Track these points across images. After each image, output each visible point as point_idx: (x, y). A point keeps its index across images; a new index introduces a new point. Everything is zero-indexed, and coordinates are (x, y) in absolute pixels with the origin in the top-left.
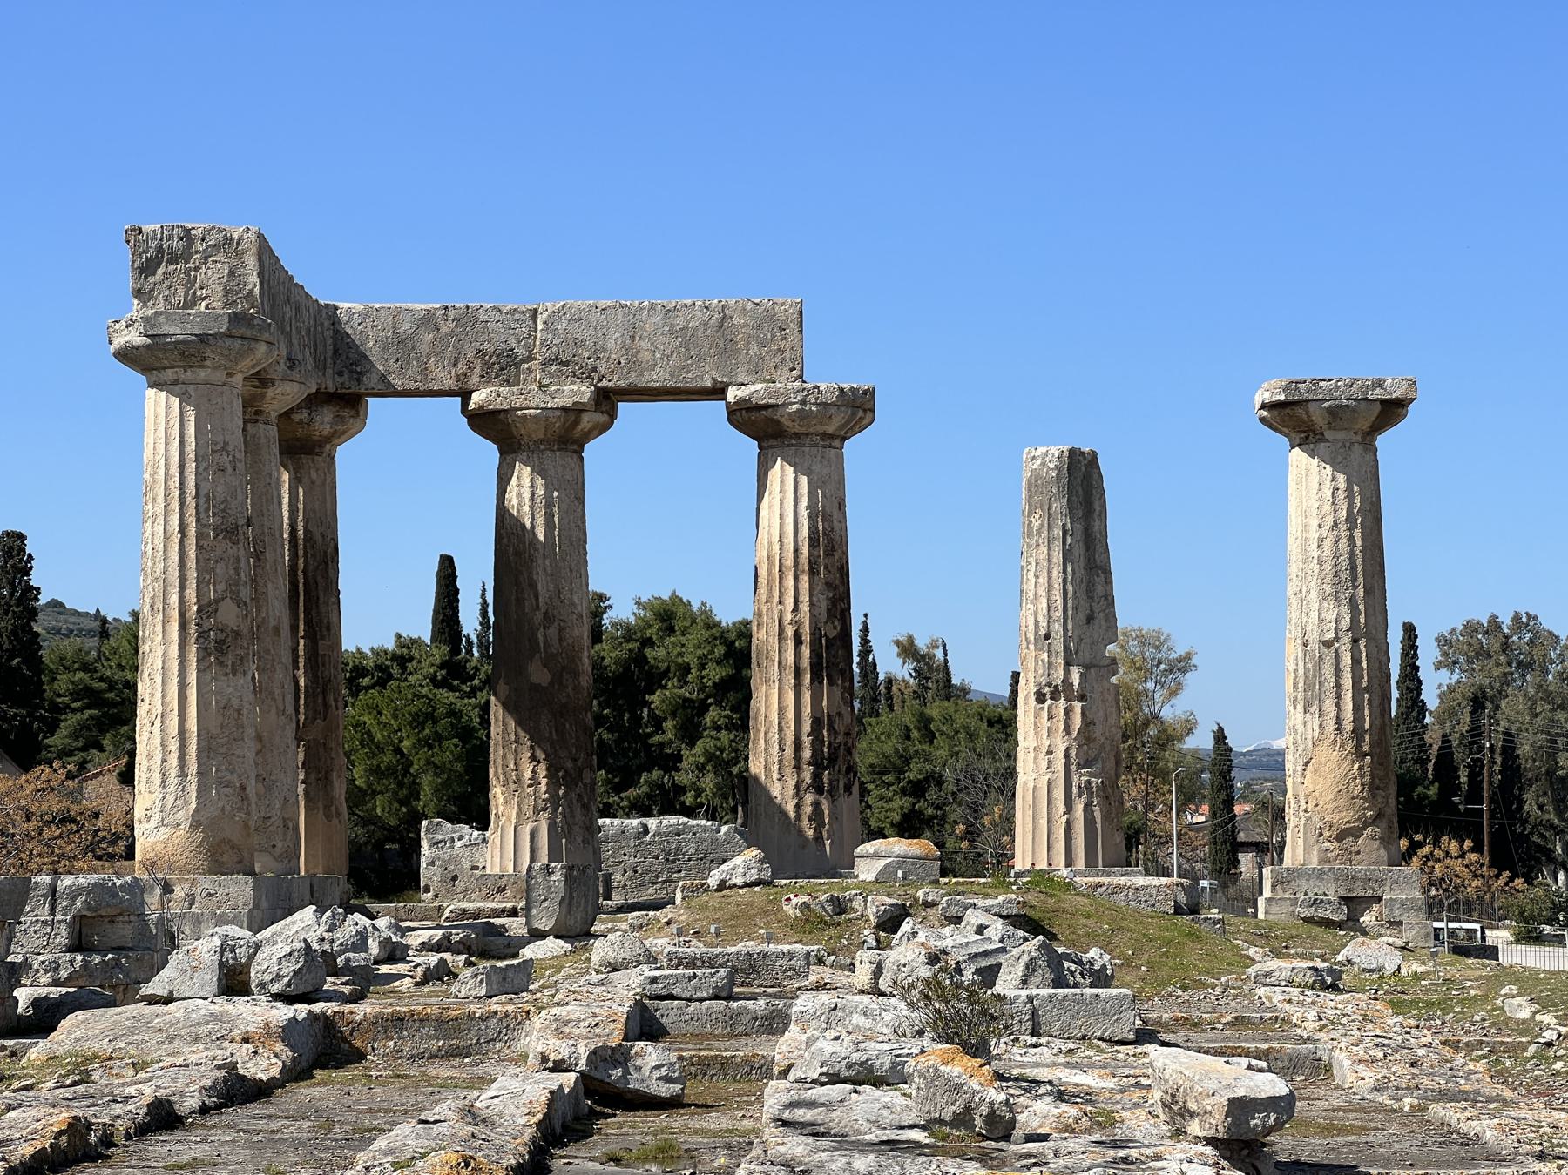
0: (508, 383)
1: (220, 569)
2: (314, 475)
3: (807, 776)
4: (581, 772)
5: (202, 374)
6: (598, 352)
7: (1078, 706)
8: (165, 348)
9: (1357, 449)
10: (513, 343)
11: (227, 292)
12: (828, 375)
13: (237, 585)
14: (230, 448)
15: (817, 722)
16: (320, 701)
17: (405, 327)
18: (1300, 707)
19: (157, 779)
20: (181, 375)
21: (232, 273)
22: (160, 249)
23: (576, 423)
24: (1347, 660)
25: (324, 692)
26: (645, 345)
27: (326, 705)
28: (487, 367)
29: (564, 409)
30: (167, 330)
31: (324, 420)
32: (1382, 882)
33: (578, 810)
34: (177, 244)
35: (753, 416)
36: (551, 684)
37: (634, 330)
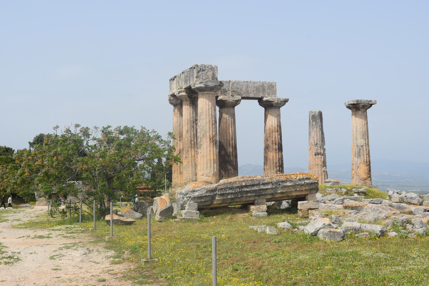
0: (225, 95)
3: (278, 169)
5: (212, 92)
6: (241, 90)
7: (323, 157)
8: (208, 88)
11: (212, 77)
12: (280, 95)
18: (356, 157)
19: (205, 168)
20: (208, 92)
21: (213, 74)
22: (201, 69)
24: (365, 149)
26: (250, 89)
29: (236, 100)
30: (209, 84)
34: (204, 68)
35: (268, 103)
37: (248, 87)
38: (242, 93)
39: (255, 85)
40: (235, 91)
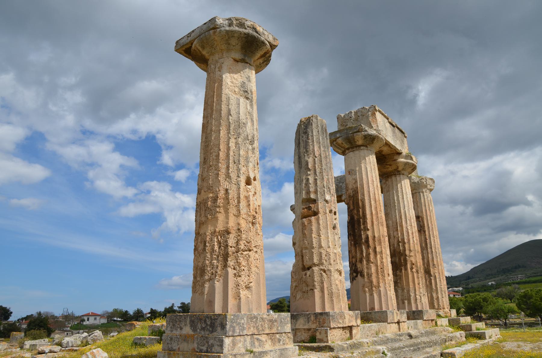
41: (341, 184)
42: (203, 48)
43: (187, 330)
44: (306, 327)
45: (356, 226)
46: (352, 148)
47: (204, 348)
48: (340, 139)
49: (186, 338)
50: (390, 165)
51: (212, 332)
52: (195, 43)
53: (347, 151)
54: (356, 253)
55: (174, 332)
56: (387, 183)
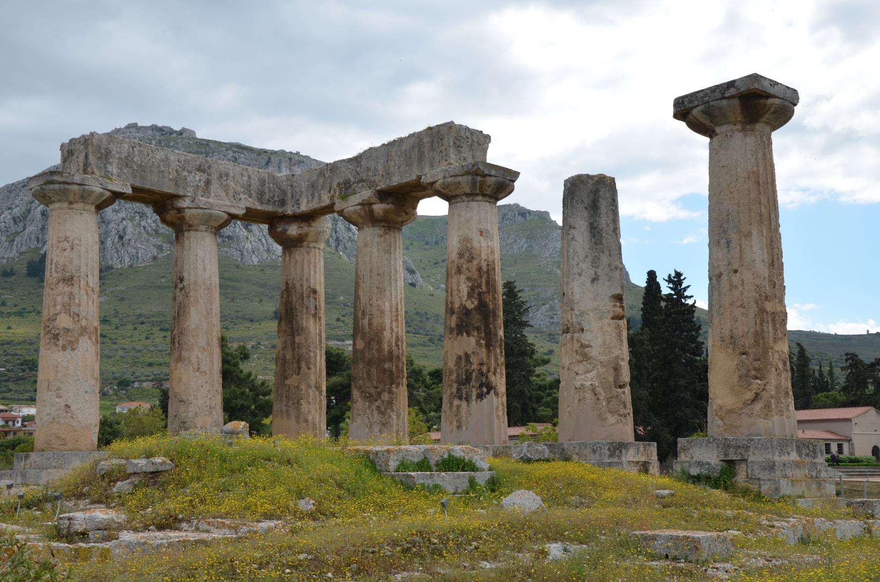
1: (59, 299)
2: (297, 257)
3: (454, 390)
4: (379, 394)
5: (57, 205)
9: (738, 136)
10: (350, 176)
13: (70, 305)
14: (70, 239)
15: (459, 358)
16: (295, 365)
17: (315, 178)
23: (371, 211)
25: (299, 361)
26: (392, 164)
27: (299, 368)
28: (341, 190)
31: (293, 230)
32: (747, 448)
33: (376, 413)
36: (364, 348)
38: (377, 179)
39: (404, 148)
40: (364, 177)
41: (185, 173)
42: (774, 112)
43: (794, 456)
44: (636, 459)
45: (491, 319)
46: (490, 197)
47: (814, 474)
48: (493, 179)
49: (797, 465)
50: (407, 214)
51: (814, 458)
52: (777, 101)
53: (480, 198)
54: (488, 357)
55: (782, 457)
56: (387, 237)
